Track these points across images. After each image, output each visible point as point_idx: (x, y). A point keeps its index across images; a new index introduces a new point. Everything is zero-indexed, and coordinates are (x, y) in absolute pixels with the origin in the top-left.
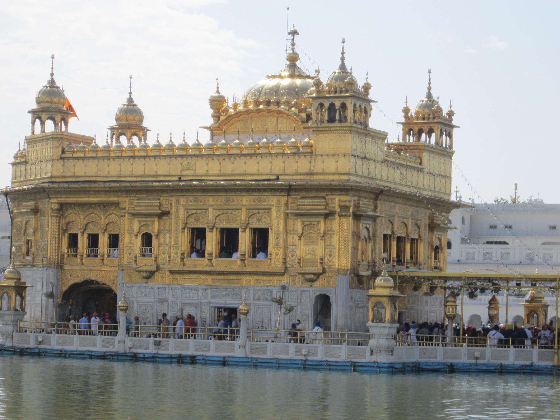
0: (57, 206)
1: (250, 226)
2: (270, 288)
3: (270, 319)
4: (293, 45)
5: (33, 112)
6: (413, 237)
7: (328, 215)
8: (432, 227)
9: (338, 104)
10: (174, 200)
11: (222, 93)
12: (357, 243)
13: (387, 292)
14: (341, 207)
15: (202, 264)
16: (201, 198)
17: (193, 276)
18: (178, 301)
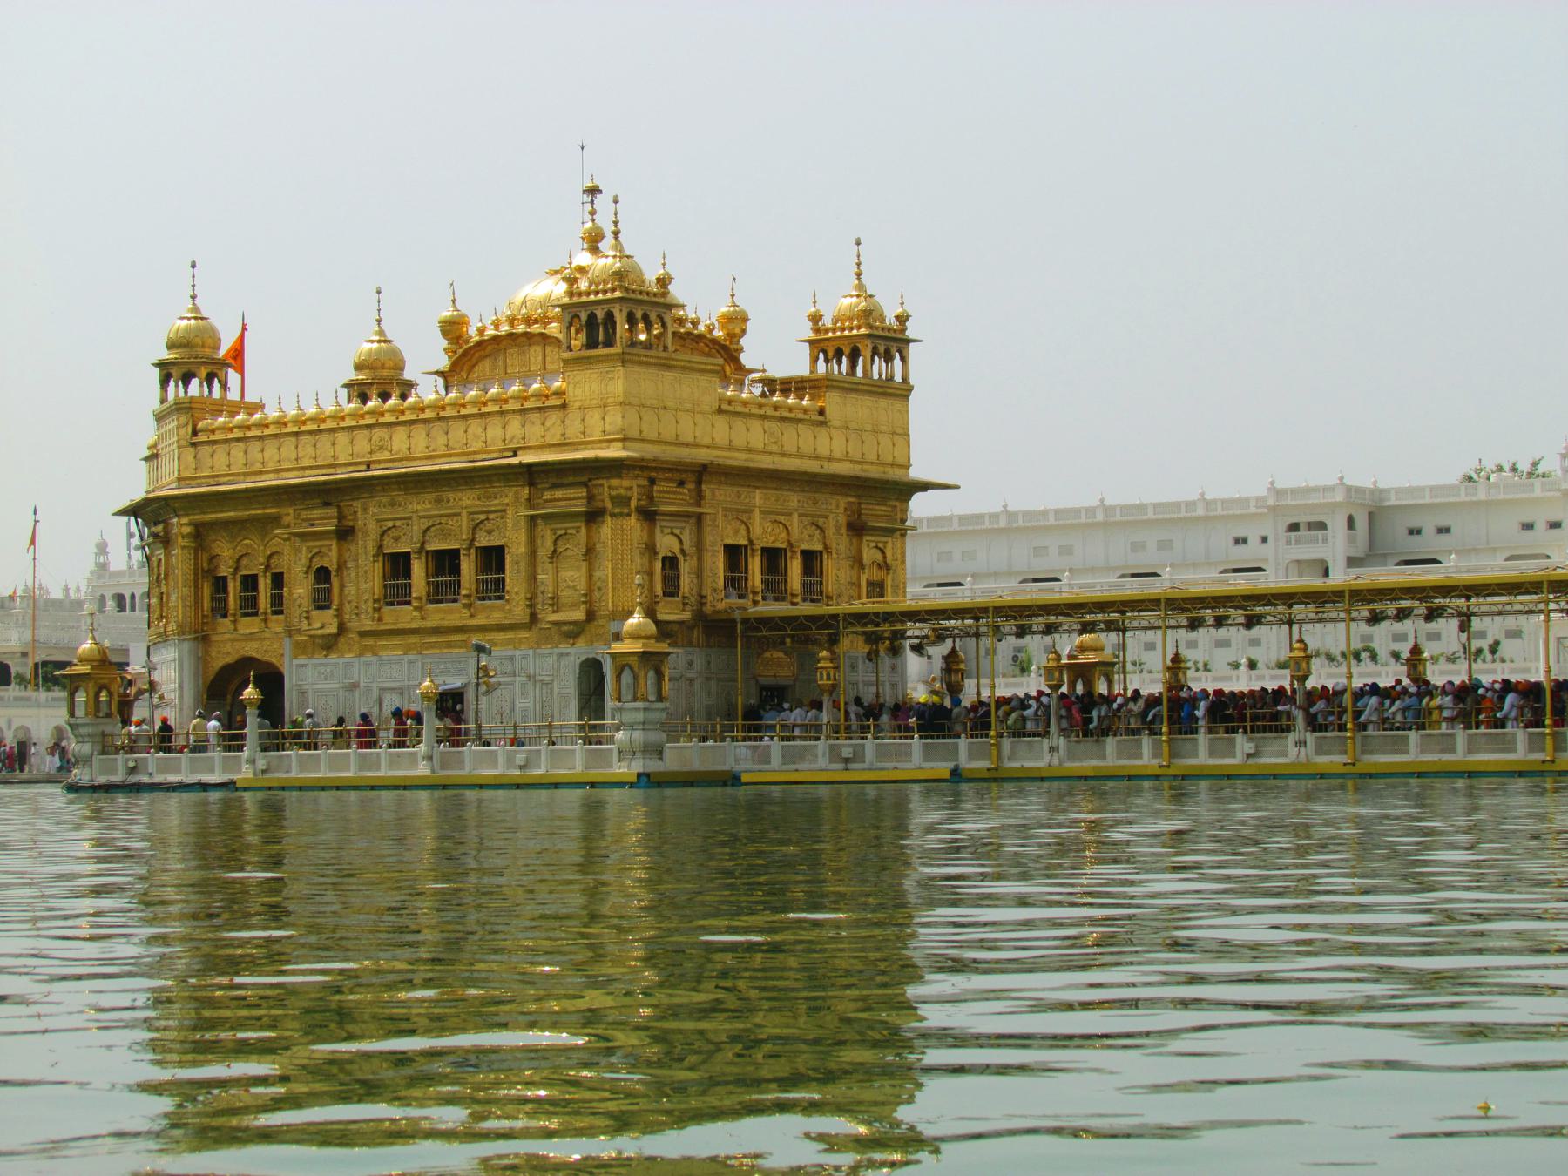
0: (187, 530)
1: (477, 544)
2: (510, 653)
3: (513, 710)
4: (593, 213)
5: (161, 365)
6: (804, 547)
7: (593, 516)
8: (857, 529)
9: (600, 314)
10: (357, 505)
11: (464, 308)
12: (651, 562)
13: (637, 647)
14: (612, 498)
15: (404, 616)
16: (401, 499)
17: (396, 641)
18: (375, 685)
